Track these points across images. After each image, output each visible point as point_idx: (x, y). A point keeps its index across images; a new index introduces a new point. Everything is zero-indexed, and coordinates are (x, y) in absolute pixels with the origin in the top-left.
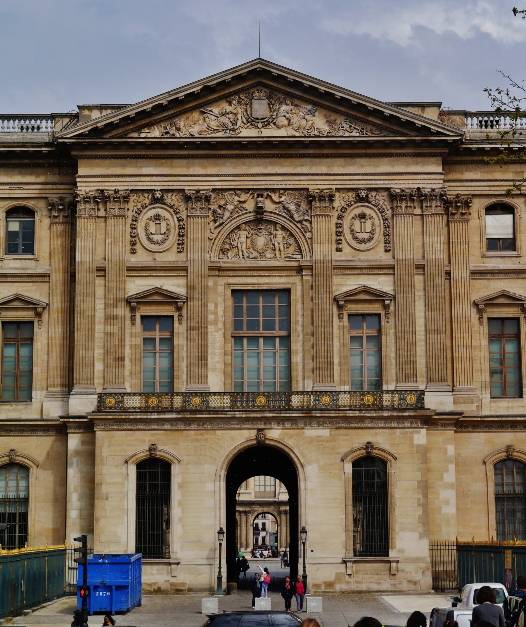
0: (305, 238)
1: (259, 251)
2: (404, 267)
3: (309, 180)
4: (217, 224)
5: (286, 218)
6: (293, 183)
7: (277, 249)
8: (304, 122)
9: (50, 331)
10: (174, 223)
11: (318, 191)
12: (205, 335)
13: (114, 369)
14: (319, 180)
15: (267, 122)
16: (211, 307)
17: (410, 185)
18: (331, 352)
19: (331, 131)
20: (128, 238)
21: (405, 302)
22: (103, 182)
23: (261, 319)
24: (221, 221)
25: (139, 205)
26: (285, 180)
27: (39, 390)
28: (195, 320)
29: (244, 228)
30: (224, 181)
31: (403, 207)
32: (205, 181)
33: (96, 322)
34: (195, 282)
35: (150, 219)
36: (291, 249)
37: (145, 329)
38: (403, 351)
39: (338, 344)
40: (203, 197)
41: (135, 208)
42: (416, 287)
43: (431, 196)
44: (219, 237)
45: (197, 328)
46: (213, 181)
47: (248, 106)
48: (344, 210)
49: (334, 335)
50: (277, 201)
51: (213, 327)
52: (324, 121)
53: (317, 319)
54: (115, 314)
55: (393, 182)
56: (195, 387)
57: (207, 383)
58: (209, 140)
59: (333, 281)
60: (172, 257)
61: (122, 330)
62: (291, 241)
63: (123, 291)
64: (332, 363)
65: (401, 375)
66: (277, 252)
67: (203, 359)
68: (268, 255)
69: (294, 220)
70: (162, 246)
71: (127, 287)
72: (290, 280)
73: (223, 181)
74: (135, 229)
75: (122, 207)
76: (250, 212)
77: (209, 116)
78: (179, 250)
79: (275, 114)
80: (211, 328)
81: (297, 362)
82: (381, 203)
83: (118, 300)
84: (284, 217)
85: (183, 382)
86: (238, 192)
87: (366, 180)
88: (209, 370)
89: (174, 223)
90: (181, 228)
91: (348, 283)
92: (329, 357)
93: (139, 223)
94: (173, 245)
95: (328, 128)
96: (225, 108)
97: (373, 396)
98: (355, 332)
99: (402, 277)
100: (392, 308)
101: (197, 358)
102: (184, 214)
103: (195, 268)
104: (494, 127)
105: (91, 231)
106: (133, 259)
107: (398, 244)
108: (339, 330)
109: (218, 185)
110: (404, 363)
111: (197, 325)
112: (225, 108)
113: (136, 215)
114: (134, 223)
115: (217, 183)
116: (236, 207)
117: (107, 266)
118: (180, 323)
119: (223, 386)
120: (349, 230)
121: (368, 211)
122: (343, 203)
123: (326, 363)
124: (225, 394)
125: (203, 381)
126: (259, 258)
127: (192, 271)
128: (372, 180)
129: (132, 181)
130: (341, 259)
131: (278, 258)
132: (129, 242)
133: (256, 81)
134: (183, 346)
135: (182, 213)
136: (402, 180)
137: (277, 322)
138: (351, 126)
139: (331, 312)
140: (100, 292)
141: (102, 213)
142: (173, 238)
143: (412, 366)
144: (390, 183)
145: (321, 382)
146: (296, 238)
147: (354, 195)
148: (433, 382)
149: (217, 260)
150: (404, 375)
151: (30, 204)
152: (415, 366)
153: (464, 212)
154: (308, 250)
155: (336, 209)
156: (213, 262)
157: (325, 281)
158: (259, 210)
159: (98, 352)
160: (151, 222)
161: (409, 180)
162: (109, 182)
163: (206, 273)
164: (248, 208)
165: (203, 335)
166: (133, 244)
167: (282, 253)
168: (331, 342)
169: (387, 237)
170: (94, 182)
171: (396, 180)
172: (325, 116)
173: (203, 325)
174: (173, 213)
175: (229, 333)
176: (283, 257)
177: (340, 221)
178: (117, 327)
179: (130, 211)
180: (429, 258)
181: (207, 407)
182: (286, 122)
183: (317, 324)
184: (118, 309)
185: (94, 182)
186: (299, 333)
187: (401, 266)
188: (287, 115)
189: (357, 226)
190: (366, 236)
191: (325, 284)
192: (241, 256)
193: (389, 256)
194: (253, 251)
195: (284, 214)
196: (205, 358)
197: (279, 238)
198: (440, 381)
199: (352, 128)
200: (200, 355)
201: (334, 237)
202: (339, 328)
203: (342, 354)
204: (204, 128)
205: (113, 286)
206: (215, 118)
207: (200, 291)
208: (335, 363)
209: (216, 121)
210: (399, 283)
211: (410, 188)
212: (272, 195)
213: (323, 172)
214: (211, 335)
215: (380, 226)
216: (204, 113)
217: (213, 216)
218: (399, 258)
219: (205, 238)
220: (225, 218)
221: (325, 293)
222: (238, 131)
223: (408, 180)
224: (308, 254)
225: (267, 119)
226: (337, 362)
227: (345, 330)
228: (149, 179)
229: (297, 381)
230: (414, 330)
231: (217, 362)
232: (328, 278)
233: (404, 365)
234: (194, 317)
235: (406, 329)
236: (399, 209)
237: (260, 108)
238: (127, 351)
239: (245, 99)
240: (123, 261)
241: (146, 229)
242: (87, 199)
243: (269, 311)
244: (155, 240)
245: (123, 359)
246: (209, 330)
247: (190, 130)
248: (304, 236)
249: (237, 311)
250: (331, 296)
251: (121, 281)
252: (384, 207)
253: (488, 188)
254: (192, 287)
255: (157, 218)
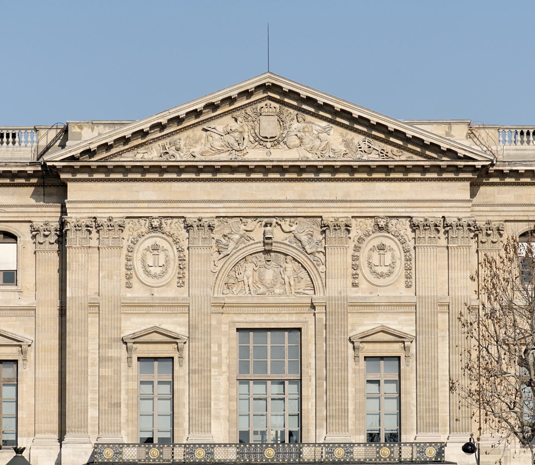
0: (318, 272)
1: (267, 285)
2: (427, 304)
3: (323, 207)
4: (222, 255)
5: (297, 249)
6: (306, 210)
7: (287, 283)
8: (317, 143)
9: (37, 371)
10: (174, 254)
11: (333, 220)
12: (209, 379)
13: (110, 416)
14: (334, 207)
15: (276, 141)
16: (214, 348)
17: (434, 214)
18: (346, 398)
19: (348, 152)
20: (124, 271)
21: (427, 344)
22: (96, 208)
23: (269, 360)
24: (225, 252)
25: (135, 234)
26: (296, 207)
27: (25, 436)
28: (197, 363)
29: (250, 260)
30: (229, 208)
31: (427, 238)
32: (208, 208)
33: (89, 364)
34: (197, 321)
35: (147, 250)
36: (303, 284)
37: (142, 371)
38: (424, 398)
39: (354, 389)
40: (206, 225)
41: (131, 237)
42: (439, 327)
43: (457, 226)
44: (223, 270)
45: (200, 371)
46: (216, 208)
47: (256, 123)
48: (360, 240)
49: (350, 380)
50: (288, 230)
51: (217, 370)
52: (341, 140)
53: (331, 362)
54: (110, 355)
55: (415, 210)
56: (197, 438)
57: (210, 431)
58: (212, 164)
59: (349, 320)
60: (172, 293)
61: (118, 372)
62: (303, 274)
63: (119, 330)
64: (346, 411)
65: (422, 423)
66: (287, 287)
67: (206, 405)
68: (277, 291)
69: (306, 252)
70: (161, 280)
71: (122, 325)
72: (302, 318)
73: (227, 208)
74: (130, 260)
75: (116, 237)
76: (257, 243)
77: (213, 134)
78: (179, 285)
79: (286, 132)
80: (214, 372)
81: (308, 409)
82: (402, 233)
83: (113, 339)
84: (294, 248)
85: (184, 430)
86: (244, 220)
87: (385, 207)
88: (212, 418)
89: (174, 254)
90: (182, 260)
91: (365, 322)
92: (343, 405)
93: (135, 255)
94: (173, 279)
95: (345, 149)
96: (230, 125)
97: (390, 449)
98: (371, 376)
99: (424, 316)
100: (413, 350)
101: (200, 404)
102: (185, 244)
103: (197, 304)
104: (531, 143)
105: (83, 263)
106: (129, 294)
107: (421, 280)
108: (355, 372)
109: (222, 212)
110: (424, 410)
111: (200, 368)
112: (230, 125)
113: (132, 245)
114: (130, 254)
115: (220, 210)
116: (242, 237)
117: (101, 302)
118: (180, 366)
119: (227, 434)
120: (367, 262)
121: (388, 242)
122: (360, 233)
123: (340, 411)
124: (231, 445)
125: (206, 429)
126: (267, 293)
127: (194, 309)
128: (392, 207)
129: (128, 208)
130: (358, 295)
131: (288, 294)
132: (124, 275)
133: (265, 95)
134: (184, 390)
135: (182, 243)
136: (425, 207)
137: (287, 363)
138: (370, 147)
139: (346, 355)
140: (93, 330)
141: (94, 243)
142: (173, 270)
143: (433, 414)
144: (413, 211)
145: (334, 431)
146: (308, 272)
147: (373, 224)
148: (456, 431)
149: (222, 295)
150: (425, 424)
151: (11, 228)
152: (437, 414)
153: (495, 240)
154: (321, 286)
155: (352, 239)
156: (217, 298)
157: (340, 320)
158: (267, 240)
159: (92, 397)
160: (148, 252)
161: (434, 207)
162: (102, 208)
163: (209, 311)
164: (255, 238)
165: (206, 379)
166: (129, 277)
167: (292, 288)
168: (346, 388)
169: (409, 271)
170: (86, 208)
171: (419, 207)
172: (341, 134)
173: (206, 368)
174: (172, 243)
175: (234, 376)
176: (293, 293)
177: (356, 254)
178: (113, 369)
179: (126, 240)
180: (454, 294)
181: (211, 459)
182: (298, 142)
183: (331, 368)
184: (113, 350)
185: (86, 208)
186: (310, 376)
187: (424, 304)
188: (299, 135)
189: (375, 260)
190: (385, 270)
191: (340, 323)
192: (248, 292)
193: (410, 293)
194: (260, 286)
195: (294, 245)
196: (209, 405)
197: (290, 271)
198: (464, 430)
199: (371, 149)
200: (203, 401)
201: (350, 271)
202: (355, 372)
203: (358, 401)
204: (207, 148)
205: (107, 324)
206: (220, 136)
207: (203, 331)
208: (349, 410)
209: (220, 140)
210: (421, 323)
211: (435, 217)
212: (282, 223)
213: (338, 199)
214: (215, 379)
215: (400, 259)
216: (207, 130)
217: (217, 246)
218: (421, 295)
219: (209, 271)
220: (230, 249)
221: (340, 334)
222: (245, 152)
223: (432, 207)
224: (321, 289)
225: (276, 138)
226: (352, 410)
227: (361, 375)
228: (146, 205)
229: (308, 430)
230: (436, 375)
231: (221, 409)
232: (343, 317)
233: (424, 413)
234: (197, 360)
235: (427, 373)
236: (422, 240)
237: (269, 126)
238: (123, 396)
239: (253, 115)
240: (119, 297)
241: (143, 261)
242: (78, 227)
243: (278, 351)
244: (153, 273)
245: (119, 405)
246: (213, 373)
247: (191, 150)
248: (317, 269)
249: (244, 351)
250: (346, 337)
251: (116, 319)
252: (406, 237)
253: (522, 214)
254: (194, 326)
255: (155, 248)
